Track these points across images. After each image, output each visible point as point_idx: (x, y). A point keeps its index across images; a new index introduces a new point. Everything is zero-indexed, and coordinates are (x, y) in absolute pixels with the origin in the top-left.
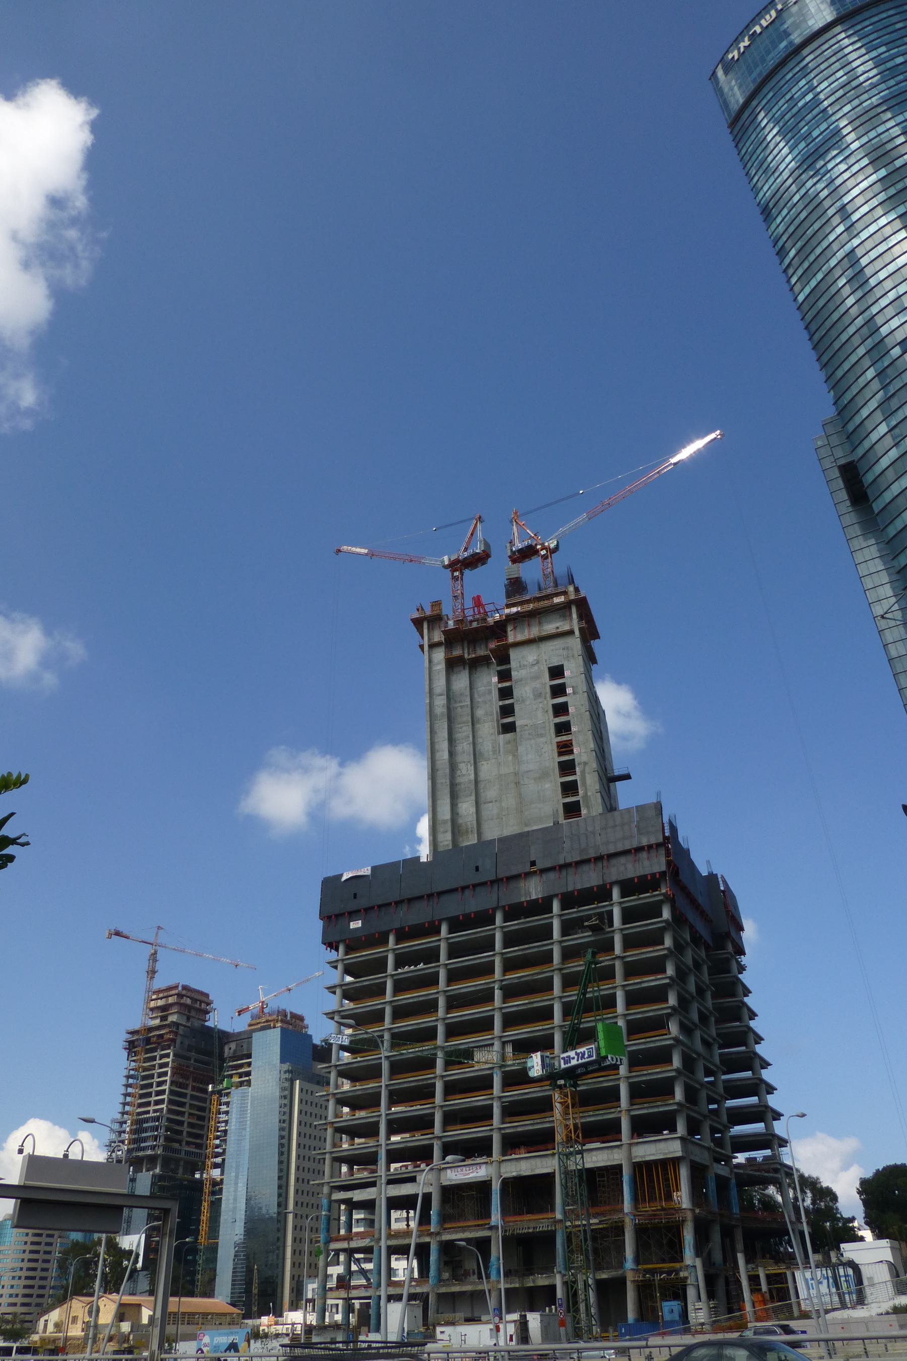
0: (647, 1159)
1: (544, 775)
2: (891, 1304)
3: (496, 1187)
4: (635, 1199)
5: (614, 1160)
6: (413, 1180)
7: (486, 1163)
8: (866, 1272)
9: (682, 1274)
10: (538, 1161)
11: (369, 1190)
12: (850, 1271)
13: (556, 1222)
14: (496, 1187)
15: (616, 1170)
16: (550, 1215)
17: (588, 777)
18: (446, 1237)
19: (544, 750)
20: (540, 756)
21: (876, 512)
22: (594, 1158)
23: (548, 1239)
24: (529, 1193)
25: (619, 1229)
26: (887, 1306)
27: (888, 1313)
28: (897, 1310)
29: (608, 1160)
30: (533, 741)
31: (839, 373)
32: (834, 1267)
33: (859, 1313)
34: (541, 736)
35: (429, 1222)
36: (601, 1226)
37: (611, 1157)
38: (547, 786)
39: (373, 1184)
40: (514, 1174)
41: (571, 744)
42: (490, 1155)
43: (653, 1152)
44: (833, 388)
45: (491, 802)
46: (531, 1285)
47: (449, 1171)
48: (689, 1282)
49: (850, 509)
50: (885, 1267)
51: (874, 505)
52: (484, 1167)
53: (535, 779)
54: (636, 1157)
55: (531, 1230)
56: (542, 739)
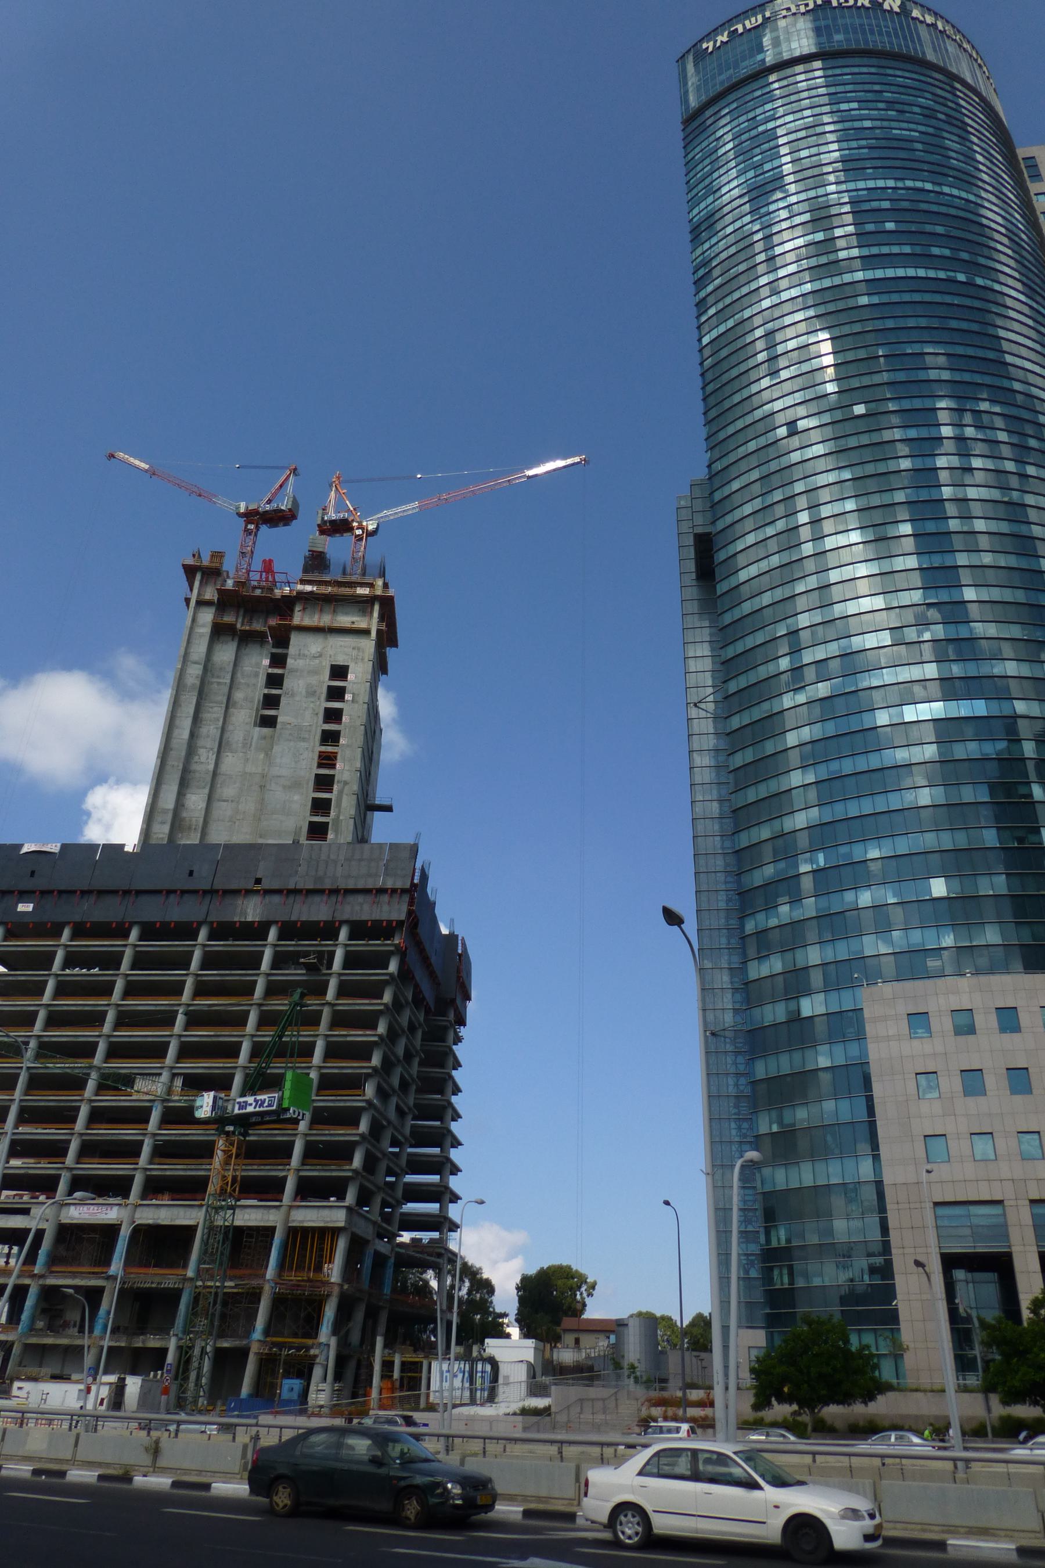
0: (306, 1224)
1: (295, 785)
2: (520, 1405)
3: (125, 1233)
4: (281, 1266)
5: (268, 1220)
6: (25, 1212)
8: (503, 1370)
9: (312, 1352)
10: (181, 1211)
12: (488, 1368)
13: (185, 1279)
14: (125, 1233)
15: (269, 1232)
16: (180, 1272)
17: (345, 798)
18: (51, 1281)
19: (302, 757)
21: (719, 593)
22: (247, 1217)
23: (172, 1297)
24: (162, 1245)
25: (255, 1296)
26: (515, 1407)
27: (515, 1414)
28: (524, 1412)
29: (261, 1220)
30: (292, 744)
31: (722, 435)
32: (473, 1362)
33: (487, 1411)
34: (304, 740)
35: (34, 1263)
36: (235, 1290)
37: (266, 1217)
38: (296, 798)
40: (150, 1222)
41: (336, 758)
42: (126, 1195)
43: (314, 1218)
44: (711, 449)
45: (227, 801)
46: (140, 1345)
47: (72, 1208)
48: (318, 1360)
49: (694, 583)
50: (524, 1368)
51: (718, 586)
52: (115, 1209)
53: (284, 787)
54: (294, 1221)
55: (154, 1286)
56: (302, 744)
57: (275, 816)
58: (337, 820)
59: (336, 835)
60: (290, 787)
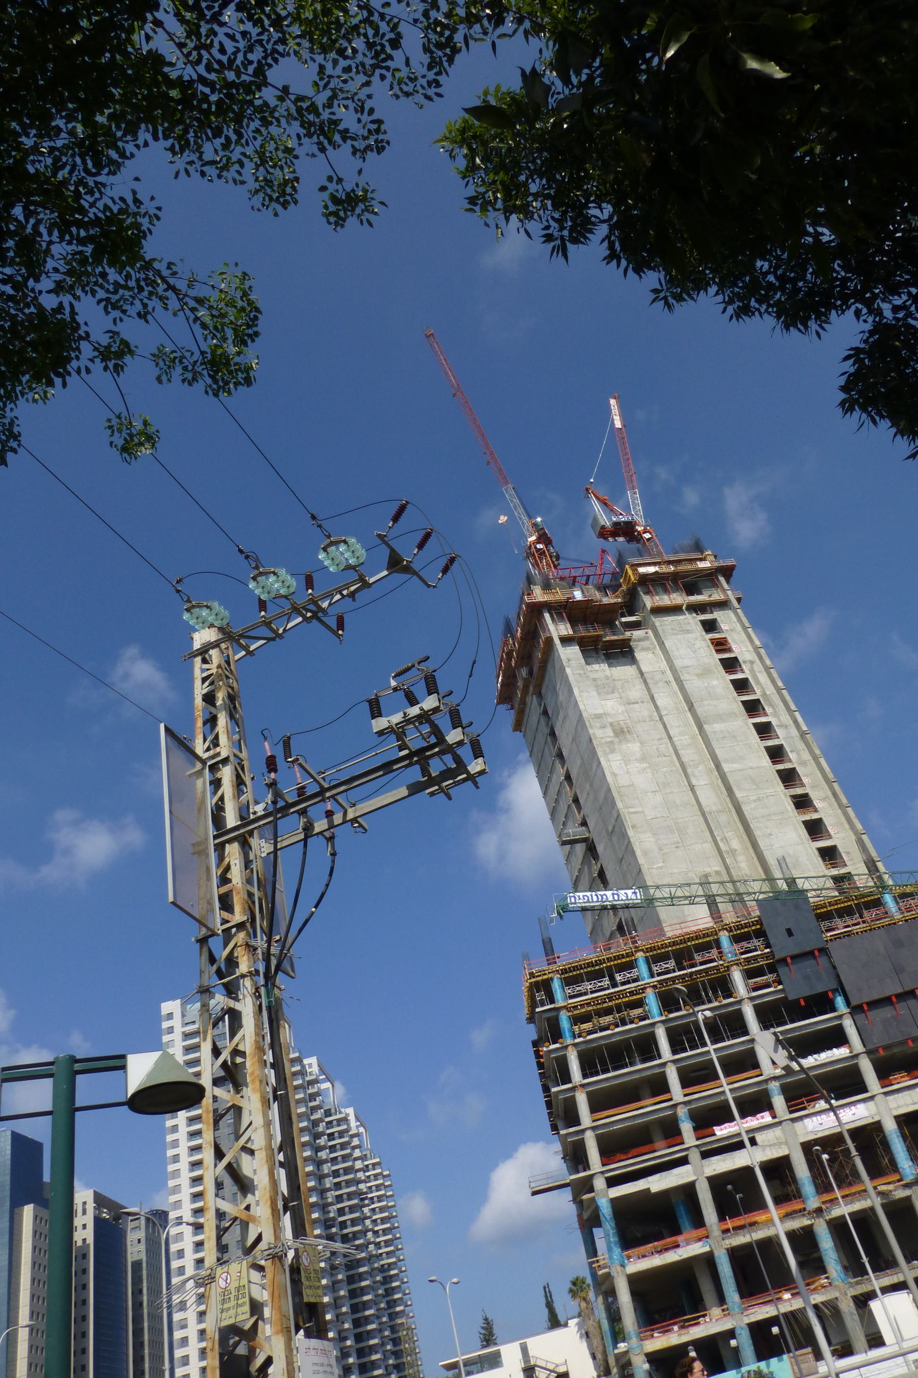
1: (705, 672)
3: (890, 1126)
7: (864, 1101)
11: (676, 1171)
17: (758, 674)
20: (694, 652)
30: (679, 637)
34: (688, 632)
35: (798, 1195)
38: (715, 682)
39: (684, 1161)
41: (726, 641)
45: (637, 703)
47: (807, 1121)
52: (861, 1107)
53: (697, 675)
57: (705, 703)
58: (764, 694)
59: (773, 708)
60: (701, 675)
